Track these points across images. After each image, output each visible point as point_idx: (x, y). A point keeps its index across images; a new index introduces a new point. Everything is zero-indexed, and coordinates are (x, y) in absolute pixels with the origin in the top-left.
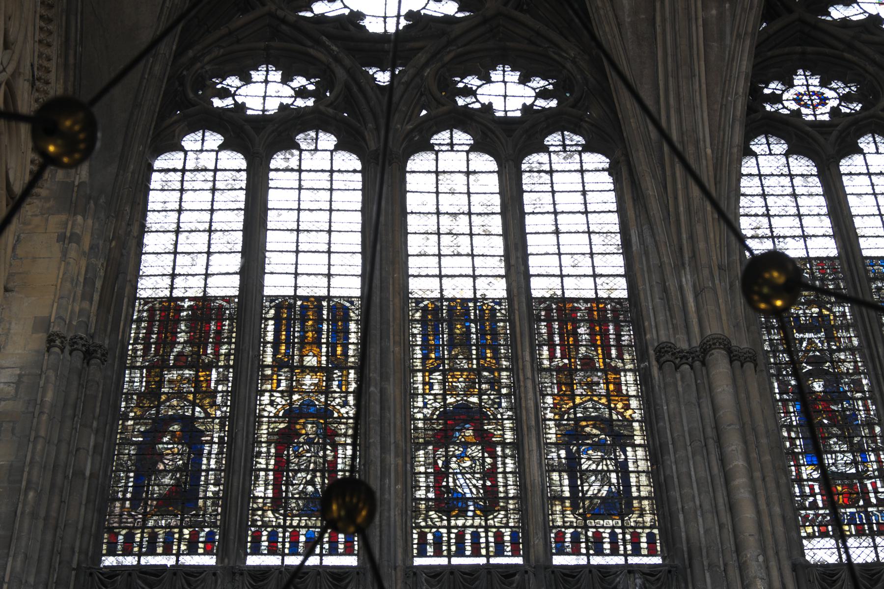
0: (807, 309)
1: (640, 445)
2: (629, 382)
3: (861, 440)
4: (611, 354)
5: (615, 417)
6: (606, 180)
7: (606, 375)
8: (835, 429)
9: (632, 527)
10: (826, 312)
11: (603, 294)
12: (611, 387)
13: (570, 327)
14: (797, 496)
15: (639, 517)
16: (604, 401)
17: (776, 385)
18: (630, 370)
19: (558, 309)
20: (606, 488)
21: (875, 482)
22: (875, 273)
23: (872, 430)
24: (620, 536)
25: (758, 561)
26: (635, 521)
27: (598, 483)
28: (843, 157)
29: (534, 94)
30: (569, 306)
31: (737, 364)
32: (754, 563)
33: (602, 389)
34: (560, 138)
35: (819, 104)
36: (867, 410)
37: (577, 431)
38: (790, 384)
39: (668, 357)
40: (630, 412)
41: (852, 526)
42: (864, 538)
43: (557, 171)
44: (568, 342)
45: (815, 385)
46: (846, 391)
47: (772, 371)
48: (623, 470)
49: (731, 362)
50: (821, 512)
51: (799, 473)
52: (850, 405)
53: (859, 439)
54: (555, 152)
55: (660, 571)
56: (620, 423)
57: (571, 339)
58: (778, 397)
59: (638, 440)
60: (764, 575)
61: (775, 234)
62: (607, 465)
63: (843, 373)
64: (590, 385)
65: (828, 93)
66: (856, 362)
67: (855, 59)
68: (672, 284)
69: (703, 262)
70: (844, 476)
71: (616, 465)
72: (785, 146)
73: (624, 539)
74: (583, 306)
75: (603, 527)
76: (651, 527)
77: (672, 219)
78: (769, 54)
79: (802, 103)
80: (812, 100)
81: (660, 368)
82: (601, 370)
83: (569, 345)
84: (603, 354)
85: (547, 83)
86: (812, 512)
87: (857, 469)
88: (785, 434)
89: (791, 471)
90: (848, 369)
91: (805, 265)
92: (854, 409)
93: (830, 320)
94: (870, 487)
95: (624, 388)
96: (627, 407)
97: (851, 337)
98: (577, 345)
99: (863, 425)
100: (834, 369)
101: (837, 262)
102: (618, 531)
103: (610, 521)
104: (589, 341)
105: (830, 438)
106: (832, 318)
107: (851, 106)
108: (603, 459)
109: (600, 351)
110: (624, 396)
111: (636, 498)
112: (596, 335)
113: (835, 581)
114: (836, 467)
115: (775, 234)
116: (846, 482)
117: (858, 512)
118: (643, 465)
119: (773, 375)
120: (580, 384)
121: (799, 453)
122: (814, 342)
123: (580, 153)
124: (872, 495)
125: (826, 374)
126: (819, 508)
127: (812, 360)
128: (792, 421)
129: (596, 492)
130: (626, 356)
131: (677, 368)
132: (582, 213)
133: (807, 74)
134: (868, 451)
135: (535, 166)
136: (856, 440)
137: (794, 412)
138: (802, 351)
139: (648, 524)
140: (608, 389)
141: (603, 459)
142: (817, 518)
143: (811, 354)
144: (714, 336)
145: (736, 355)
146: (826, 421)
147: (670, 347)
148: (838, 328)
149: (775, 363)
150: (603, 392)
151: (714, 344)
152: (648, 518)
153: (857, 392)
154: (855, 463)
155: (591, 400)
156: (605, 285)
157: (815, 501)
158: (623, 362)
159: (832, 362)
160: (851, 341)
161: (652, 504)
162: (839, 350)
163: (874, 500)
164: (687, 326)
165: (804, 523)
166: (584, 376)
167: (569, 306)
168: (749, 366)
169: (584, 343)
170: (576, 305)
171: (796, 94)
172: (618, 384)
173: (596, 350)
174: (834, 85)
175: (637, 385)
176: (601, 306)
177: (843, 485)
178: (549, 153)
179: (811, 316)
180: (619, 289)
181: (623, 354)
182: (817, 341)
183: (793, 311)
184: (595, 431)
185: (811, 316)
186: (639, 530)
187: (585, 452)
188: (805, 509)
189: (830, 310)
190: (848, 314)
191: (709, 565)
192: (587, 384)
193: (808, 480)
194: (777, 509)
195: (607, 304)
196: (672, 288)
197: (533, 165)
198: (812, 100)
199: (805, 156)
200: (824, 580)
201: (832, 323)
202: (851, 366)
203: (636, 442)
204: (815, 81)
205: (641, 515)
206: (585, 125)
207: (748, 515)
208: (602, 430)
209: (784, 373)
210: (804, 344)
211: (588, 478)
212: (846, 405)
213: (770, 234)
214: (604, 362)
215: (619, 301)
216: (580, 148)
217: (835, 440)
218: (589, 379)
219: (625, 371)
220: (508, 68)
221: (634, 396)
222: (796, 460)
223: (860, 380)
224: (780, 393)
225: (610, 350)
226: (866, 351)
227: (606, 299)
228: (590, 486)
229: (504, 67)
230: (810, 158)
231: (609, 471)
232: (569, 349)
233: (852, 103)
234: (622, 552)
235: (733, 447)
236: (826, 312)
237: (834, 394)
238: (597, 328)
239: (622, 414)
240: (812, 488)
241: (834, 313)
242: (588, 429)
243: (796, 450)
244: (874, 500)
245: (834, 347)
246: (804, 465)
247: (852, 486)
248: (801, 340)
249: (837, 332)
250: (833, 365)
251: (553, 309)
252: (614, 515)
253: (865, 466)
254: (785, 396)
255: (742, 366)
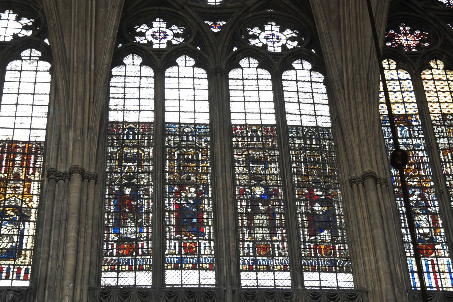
0: (132, 150)
1: (32, 221)
2: (35, 188)
3: (142, 221)
4: (29, 172)
5: (23, 206)
6: (47, 77)
7: (24, 183)
8: (131, 214)
9: (18, 265)
10: (140, 152)
11: (32, 139)
12: (26, 189)
13: (12, 157)
14: (104, 250)
15: (23, 260)
16: (20, 197)
17: (107, 190)
18: (37, 181)
19: (9, 147)
20: (11, 244)
21: (143, 243)
22: (169, 132)
23: (148, 215)
24: (12, 270)
25: (69, 287)
26: (21, 262)
27: (7, 241)
28: (168, 67)
29: (21, 27)
30: (14, 145)
31: (86, 180)
32: (67, 288)
33: (20, 191)
34: (29, 52)
35: (163, 38)
36: (148, 205)
37: (3, 213)
38: (114, 190)
39: (52, 176)
40: (32, 203)
41: (127, 266)
42: (131, 272)
43: (24, 71)
44: (9, 164)
45: (126, 191)
46: (140, 195)
47: (107, 183)
48: (21, 234)
49: (83, 179)
50: (114, 258)
51: (108, 237)
52: (141, 202)
53: (141, 220)
54: (25, 60)
55: (23, 290)
56: (25, 209)
57: (11, 163)
58: (107, 196)
59: (32, 219)
60: (71, 294)
61: (125, 109)
62: (14, 232)
63: (141, 185)
64: (15, 188)
65: (169, 32)
66: (149, 179)
67: (183, 15)
68: (63, 136)
69: (78, 126)
70: (130, 239)
71: (18, 232)
72: (141, 61)
73: (13, 271)
74: (21, 145)
75: (4, 265)
76: (28, 265)
77: (70, 102)
78: (142, 10)
79: (155, 37)
80: (160, 36)
81: (49, 181)
82: (22, 180)
83: (9, 166)
84: (25, 172)
85: (29, 21)
86: (110, 258)
87: (136, 235)
88: (106, 216)
89: (105, 236)
90: (144, 183)
91: (136, 126)
92: (142, 204)
93: (142, 156)
94: (140, 246)
95: (32, 190)
96: (31, 201)
97: (149, 166)
98: (13, 166)
99: (144, 213)
100: (137, 182)
101: (152, 125)
102: (11, 267)
103: (9, 261)
104: (20, 164)
105: (127, 219)
106: (143, 155)
107: (178, 40)
108: (12, 228)
109: (24, 170)
110: (31, 194)
111: (24, 250)
112: (24, 161)
113: (107, 297)
114: (127, 235)
115: (125, 109)
116: (130, 243)
117: (132, 259)
118: (32, 232)
119: (107, 185)
120: (10, 187)
121: (110, 227)
122: (131, 168)
123: (37, 61)
124: (140, 250)
125: (133, 185)
126: (113, 256)
127: (128, 177)
128: (111, 210)
129: (5, 246)
130: (37, 173)
131: (57, 181)
132: (32, 94)
133: (161, 21)
134: (144, 226)
135: (14, 68)
136: (139, 220)
137: (113, 205)
138: (124, 172)
139: (27, 264)
140: (23, 191)
141: (12, 228)
142: (112, 261)
143: (128, 174)
144: (75, 167)
145: (86, 176)
146: (127, 210)
147: (54, 171)
148: (144, 160)
149: (110, 179)
150: (21, 192)
151: (74, 171)
152: (27, 260)
153: (146, 195)
154: (136, 233)
155: (14, 196)
156: (35, 134)
157: (112, 252)
158: (34, 177)
159: (137, 179)
160: (149, 168)
161: (31, 253)
162: (142, 172)
163: (140, 253)
164: (67, 159)
165: (105, 263)
166: (13, 184)
167: (14, 145)
168: (93, 182)
169: (17, 165)
170: (18, 144)
171: (153, 32)
172: (29, 188)
173: (22, 170)
174: (172, 28)
175: (39, 188)
176: (30, 145)
177: (127, 244)
178: (22, 60)
179: (133, 154)
180: (41, 137)
181: (35, 172)
182: (133, 167)
183: (125, 150)
184: (12, 213)
185: (133, 154)
186: (21, 267)
187: (4, 225)
188: (107, 256)
189: (143, 151)
190: (151, 153)
191: (49, 287)
192: (14, 188)
193: (112, 241)
194: (88, 258)
195: (33, 145)
196: (63, 139)
197: (12, 67)
198: (160, 36)
199: (149, 66)
200: (102, 296)
201: (142, 158)
202: (145, 181)
203: (31, 220)
204: (164, 25)
205: (25, 259)
206: (41, 46)
207: (70, 263)
208: (16, 213)
209: (113, 184)
210: (126, 169)
211: (3, 238)
212: (139, 202)
213: (123, 109)
214: (25, 176)
215: (40, 143)
216: (38, 58)
217: (129, 220)
218: (15, 185)
219: (34, 181)
220: (11, 12)
221: (36, 195)
222: (108, 230)
223: (148, 189)
224: (109, 195)
225: (29, 169)
226: (154, 173)
227: (34, 142)
228: (3, 242)
229: (9, 11)
230: (152, 68)
231: (14, 235)
232: (9, 168)
233: (179, 38)
234: (11, 278)
235: (71, 226)
236: (140, 152)
237: (135, 196)
238: (25, 158)
239: (27, 204)
240: (112, 245)
241: (144, 152)
242: (8, 212)
243: (109, 225)
244: (140, 253)
245: (140, 171)
246: (112, 233)
247: (132, 245)
248: (126, 166)
249: (144, 163)
250: (137, 180)
251: (5, 147)
252: (12, 258)
253: (140, 235)
254: (111, 197)
255: (89, 181)
